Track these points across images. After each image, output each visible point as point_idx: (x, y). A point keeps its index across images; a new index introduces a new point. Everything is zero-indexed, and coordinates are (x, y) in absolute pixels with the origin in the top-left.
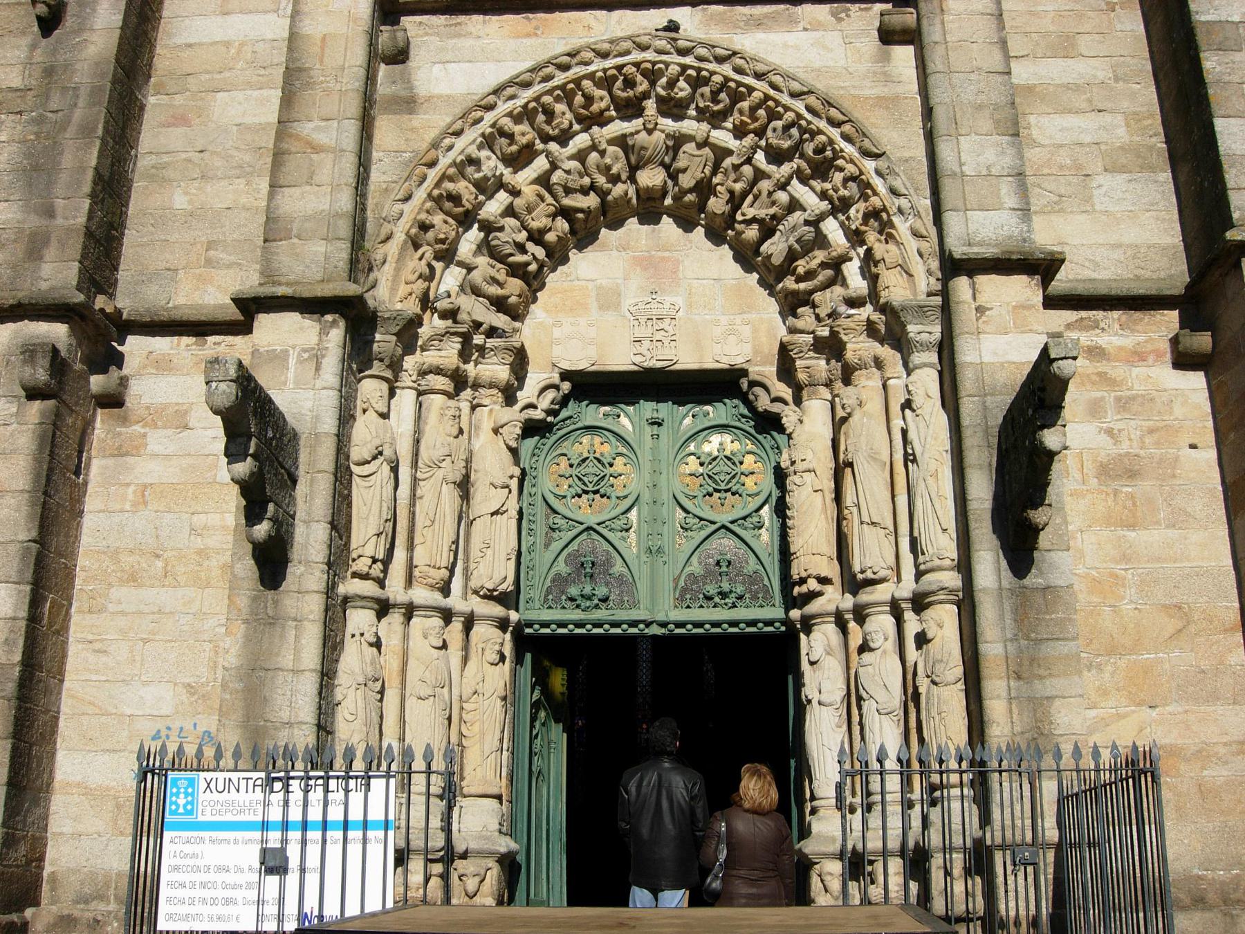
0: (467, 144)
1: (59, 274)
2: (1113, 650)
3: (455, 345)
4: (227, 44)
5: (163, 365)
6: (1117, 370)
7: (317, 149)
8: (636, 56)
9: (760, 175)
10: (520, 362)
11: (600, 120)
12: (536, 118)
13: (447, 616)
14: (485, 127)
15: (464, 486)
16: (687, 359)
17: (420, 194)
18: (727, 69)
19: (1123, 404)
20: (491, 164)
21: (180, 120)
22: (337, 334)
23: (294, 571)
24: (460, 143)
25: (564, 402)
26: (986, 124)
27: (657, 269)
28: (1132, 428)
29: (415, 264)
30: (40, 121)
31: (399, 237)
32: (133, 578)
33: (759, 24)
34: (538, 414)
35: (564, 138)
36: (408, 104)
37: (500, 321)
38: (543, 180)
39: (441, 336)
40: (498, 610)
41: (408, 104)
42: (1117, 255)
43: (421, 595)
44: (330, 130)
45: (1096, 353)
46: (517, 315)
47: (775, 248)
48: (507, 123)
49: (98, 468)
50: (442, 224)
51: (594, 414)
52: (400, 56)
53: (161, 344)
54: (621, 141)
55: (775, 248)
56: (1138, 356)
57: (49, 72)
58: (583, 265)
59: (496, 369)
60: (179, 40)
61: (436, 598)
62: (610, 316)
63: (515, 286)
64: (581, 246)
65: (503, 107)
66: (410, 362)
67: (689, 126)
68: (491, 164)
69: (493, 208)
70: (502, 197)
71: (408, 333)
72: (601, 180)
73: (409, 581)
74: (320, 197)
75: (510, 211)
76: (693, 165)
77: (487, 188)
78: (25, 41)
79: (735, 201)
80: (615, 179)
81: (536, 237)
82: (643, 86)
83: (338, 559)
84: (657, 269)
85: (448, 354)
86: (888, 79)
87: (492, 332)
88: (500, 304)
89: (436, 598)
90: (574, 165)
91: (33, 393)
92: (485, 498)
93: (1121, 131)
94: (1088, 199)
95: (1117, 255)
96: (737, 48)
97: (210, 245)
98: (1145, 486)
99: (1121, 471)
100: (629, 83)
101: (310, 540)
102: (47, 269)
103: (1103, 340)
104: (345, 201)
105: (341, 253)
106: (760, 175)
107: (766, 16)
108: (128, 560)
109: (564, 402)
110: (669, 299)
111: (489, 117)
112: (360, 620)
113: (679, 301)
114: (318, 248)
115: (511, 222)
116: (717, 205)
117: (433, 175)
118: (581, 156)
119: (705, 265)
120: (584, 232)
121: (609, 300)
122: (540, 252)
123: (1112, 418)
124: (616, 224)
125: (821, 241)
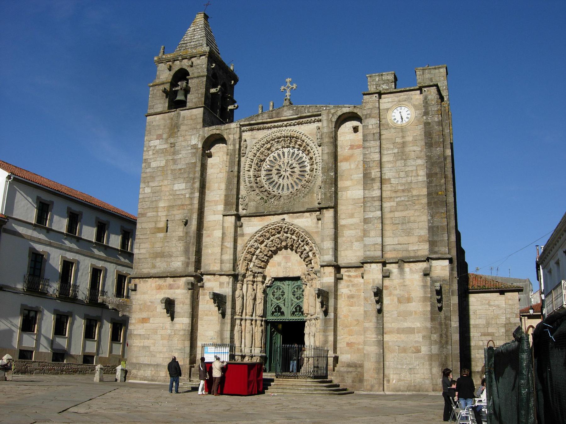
0: (252, 242)
1: (191, 269)
2: (347, 327)
3: (252, 277)
4: (215, 221)
5: (209, 280)
6: (352, 279)
7: (227, 248)
8: (278, 225)
9: (300, 244)
10: (264, 277)
11: (274, 235)
12: (263, 236)
13: (252, 320)
14: (254, 239)
15: (255, 299)
16: (291, 275)
17: (245, 252)
18: (292, 227)
19: (353, 285)
20: (256, 245)
21: (209, 236)
22: (231, 279)
23: (226, 316)
24: (251, 242)
25: (273, 282)
26: (328, 239)
27: (287, 259)
28: (354, 289)
29: (245, 264)
30: (186, 242)
31: (242, 260)
32: (207, 315)
33: (297, 217)
34: (268, 285)
35: (268, 239)
36: (243, 235)
37: (260, 270)
38: (266, 246)
39: (250, 275)
40: (261, 318)
41: (243, 235)
42: (355, 258)
43: (248, 317)
44: (229, 244)
45: (349, 276)
46: (264, 268)
47: (303, 256)
48: (258, 238)
49: (201, 297)
50: (249, 256)
51: (278, 283)
52: (241, 226)
53: (209, 277)
54: (278, 238)
55: (303, 256)
56: (356, 277)
57: (187, 233)
58: (276, 258)
59: (260, 279)
60: (208, 220)
61: (251, 318)
62: (279, 268)
63: (263, 263)
64: (275, 254)
65: (257, 235)
66: (245, 280)
67: (289, 235)
68: (256, 245)
69: (258, 252)
70: (259, 249)
71: (244, 276)
72: (276, 244)
73: (246, 315)
74: (228, 256)
75: (261, 252)
76: (289, 242)
77: (257, 248)
78: (182, 227)
79: (297, 248)
80: (278, 244)
81: (266, 255)
82: (280, 229)
83: (233, 313)
84: (287, 259)
85: (251, 278)
86: (318, 227)
87: (259, 273)
88: (261, 267)
89: (251, 318)
90: (271, 243)
91: (189, 289)
92: (258, 301)
93: (360, 233)
94: (352, 247)
95: (355, 258)
96: (293, 223)
97: (215, 259)
98: (355, 300)
99: (351, 297)
100: (277, 229)
101: (229, 311)
102: (190, 268)
103: (351, 274)
104: (232, 257)
105: (232, 266)
106: (300, 244)
107: (299, 216)
108: (206, 312)
109: (273, 282)
110: (288, 264)
111: (255, 237)
112: (238, 322)
113: (290, 264)
114: (228, 265)
115: (261, 254)
116: (294, 248)
117: (247, 248)
118: (272, 241)
119: (295, 257)
120: (275, 252)
121: (279, 264)
122: (267, 258)
123: (351, 288)
124: (281, 250)
125: (308, 256)
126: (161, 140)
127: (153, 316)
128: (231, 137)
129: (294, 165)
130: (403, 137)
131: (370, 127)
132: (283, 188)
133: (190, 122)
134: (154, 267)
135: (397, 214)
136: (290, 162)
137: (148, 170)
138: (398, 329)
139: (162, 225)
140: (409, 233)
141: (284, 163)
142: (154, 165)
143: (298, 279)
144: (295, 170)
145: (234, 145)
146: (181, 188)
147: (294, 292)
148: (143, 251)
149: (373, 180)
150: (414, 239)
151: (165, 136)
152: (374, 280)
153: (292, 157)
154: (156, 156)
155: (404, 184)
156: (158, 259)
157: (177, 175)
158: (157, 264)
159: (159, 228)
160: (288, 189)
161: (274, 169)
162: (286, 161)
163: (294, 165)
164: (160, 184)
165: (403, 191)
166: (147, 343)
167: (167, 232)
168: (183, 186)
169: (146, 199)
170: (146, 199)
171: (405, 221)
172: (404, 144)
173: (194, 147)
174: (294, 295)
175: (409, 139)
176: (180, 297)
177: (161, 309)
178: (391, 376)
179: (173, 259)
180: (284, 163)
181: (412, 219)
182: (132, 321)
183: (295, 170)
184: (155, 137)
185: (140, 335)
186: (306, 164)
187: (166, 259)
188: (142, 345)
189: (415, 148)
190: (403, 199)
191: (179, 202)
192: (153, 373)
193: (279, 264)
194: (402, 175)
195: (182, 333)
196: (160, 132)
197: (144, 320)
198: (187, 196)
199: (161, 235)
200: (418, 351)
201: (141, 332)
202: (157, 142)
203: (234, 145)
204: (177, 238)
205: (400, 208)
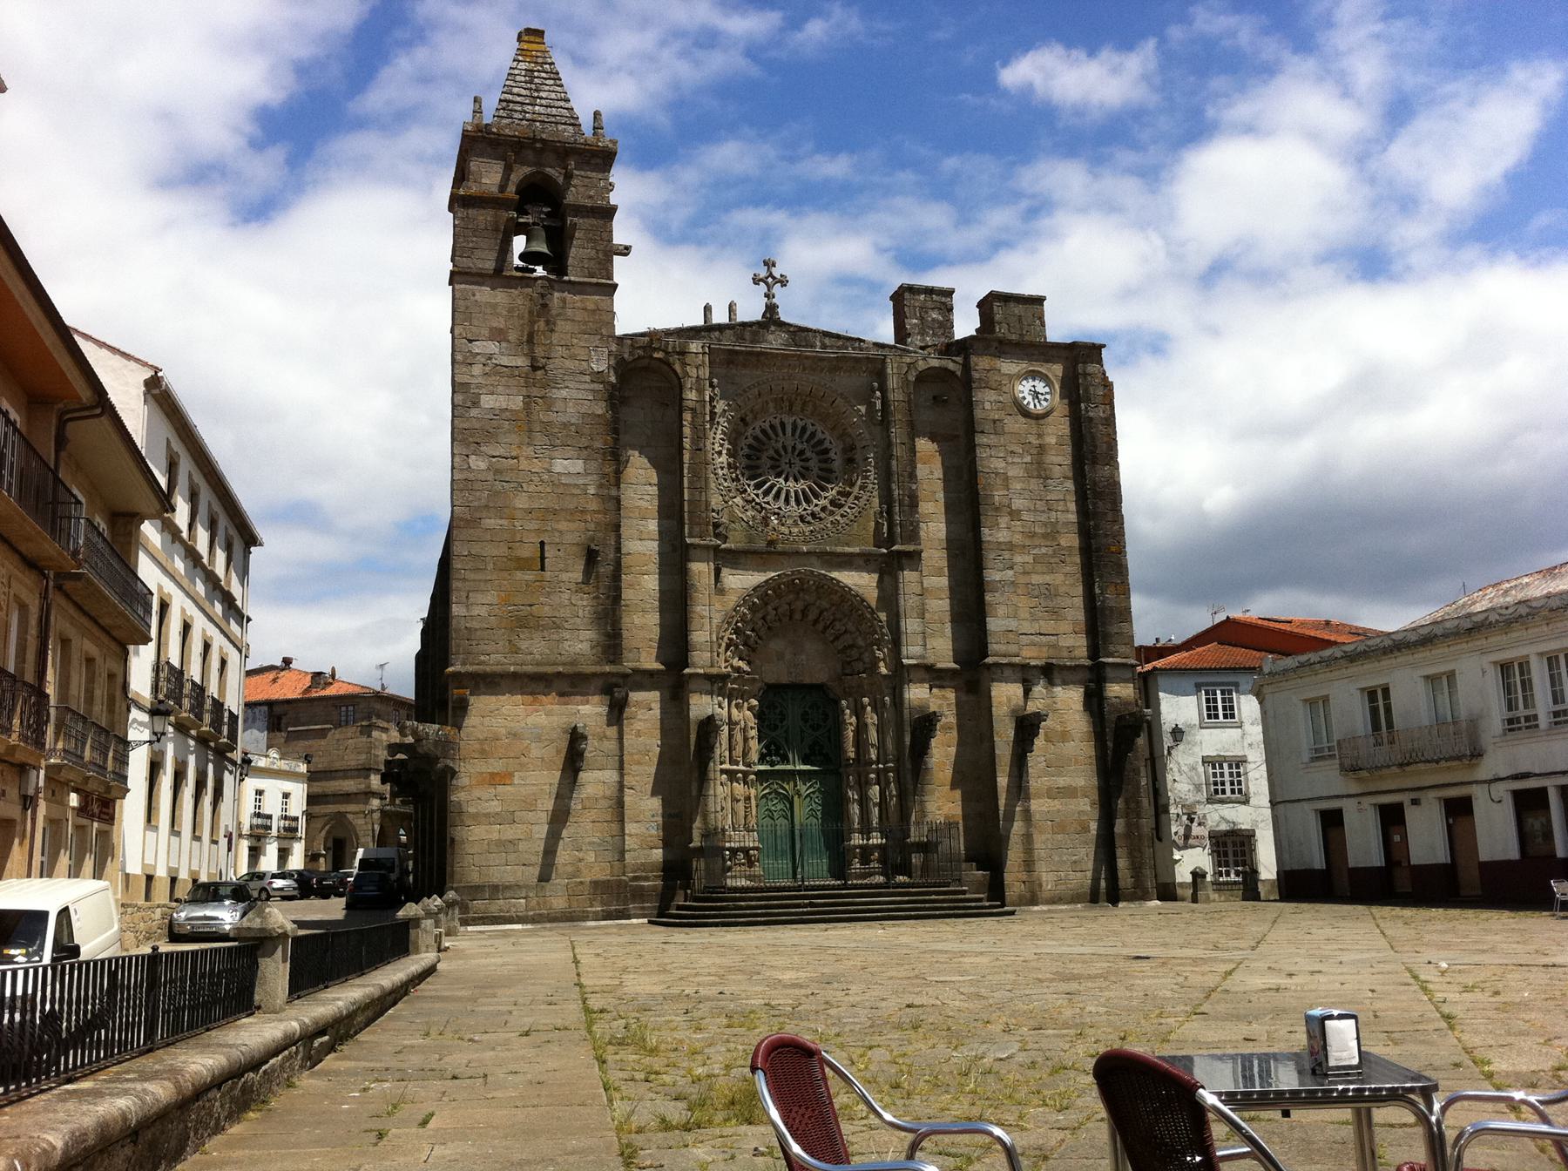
15: (744, 730)
16: (807, 681)
30: (596, 598)
32: (639, 763)
38: (764, 618)
47: (840, 645)
55: (840, 645)
116: (820, 627)
119: (812, 647)
121: (780, 656)
126: (504, 344)
127: (522, 767)
128: (693, 372)
129: (808, 454)
130: (1040, 436)
131: (987, 406)
132: (787, 501)
133: (579, 316)
134: (516, 650)
135: (1036, 579)
136: (799, 447)
137: (474, 412)
138: (1049, 789)
139: (528, 551)
140: (1055, 613)
141: (784, 448)
142: (488, 401)
143: (819, 688)
144: (811, 464)
145: (700, 391)
146: (572, 470)
147: (806, 713)
148: (476, 611)
149: (997, 509)
150: (1065, 627)
151: (513, 336)
152: (1009, 700)
153: (801, 437)
154: (490, 380)
155: (1045, 525)
156: (525, 634)
157: (556, 437)
158: (524, 645)
159: (518, 559)
160: (798, 503)
161: (764, 457)
162: (790, 443)
163: (808, 454)
164: (514, 454)
165: (1045, 536)
166: (510, 832)
167: (543, 569)
168: (578, 466)
169: (477, 486)
170: (477, 486)
171: (1049, 592)
172: (1042, 449)
173: (597, 377)
174: (806, 721)
175: (1051, 440)
176: (591, 722)
177: (555, 753)
178: (1044, 877)
179: (566, 635)
180: (784, 448)
181: (1062, 590)
182: (463, 781)
183: (811, 464)
184: (486, 332)
185: (487, 815)
186: (832, 454)
187: (546, 633)
188: (495, 836)
189: (1059, 459)
190: (1044, 550)
191: (570, 504)
192: (534, 903)
193: (780, 656)
194: (1040, 505)
195: (604, 803)
196: (499, 323)
197: (496, 779)
198: (592, 491)
199: (529, 576)
200: (1086, 829)
201: (495, 807)
202: (492, 347)
203: (700, 391)
204: (573, 587)
205: (1039, 568)
